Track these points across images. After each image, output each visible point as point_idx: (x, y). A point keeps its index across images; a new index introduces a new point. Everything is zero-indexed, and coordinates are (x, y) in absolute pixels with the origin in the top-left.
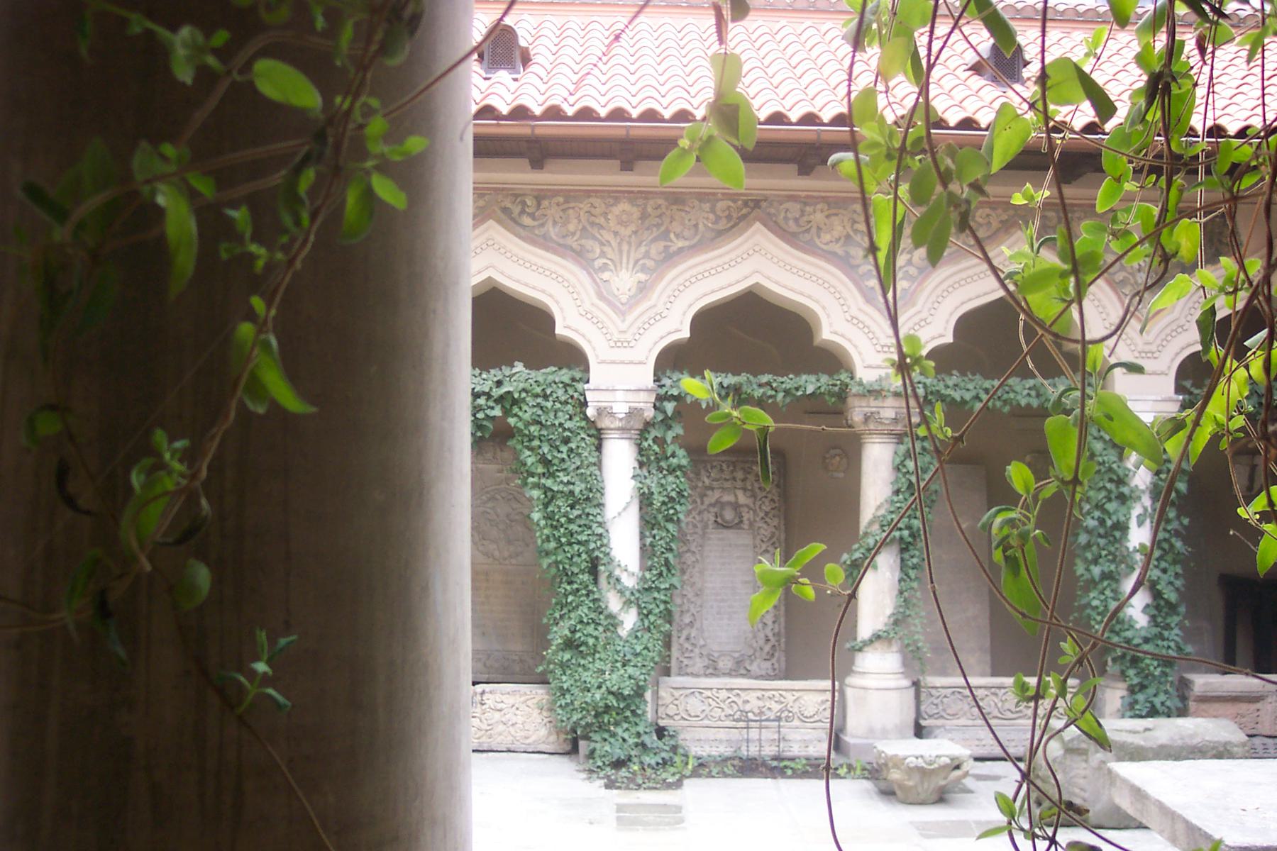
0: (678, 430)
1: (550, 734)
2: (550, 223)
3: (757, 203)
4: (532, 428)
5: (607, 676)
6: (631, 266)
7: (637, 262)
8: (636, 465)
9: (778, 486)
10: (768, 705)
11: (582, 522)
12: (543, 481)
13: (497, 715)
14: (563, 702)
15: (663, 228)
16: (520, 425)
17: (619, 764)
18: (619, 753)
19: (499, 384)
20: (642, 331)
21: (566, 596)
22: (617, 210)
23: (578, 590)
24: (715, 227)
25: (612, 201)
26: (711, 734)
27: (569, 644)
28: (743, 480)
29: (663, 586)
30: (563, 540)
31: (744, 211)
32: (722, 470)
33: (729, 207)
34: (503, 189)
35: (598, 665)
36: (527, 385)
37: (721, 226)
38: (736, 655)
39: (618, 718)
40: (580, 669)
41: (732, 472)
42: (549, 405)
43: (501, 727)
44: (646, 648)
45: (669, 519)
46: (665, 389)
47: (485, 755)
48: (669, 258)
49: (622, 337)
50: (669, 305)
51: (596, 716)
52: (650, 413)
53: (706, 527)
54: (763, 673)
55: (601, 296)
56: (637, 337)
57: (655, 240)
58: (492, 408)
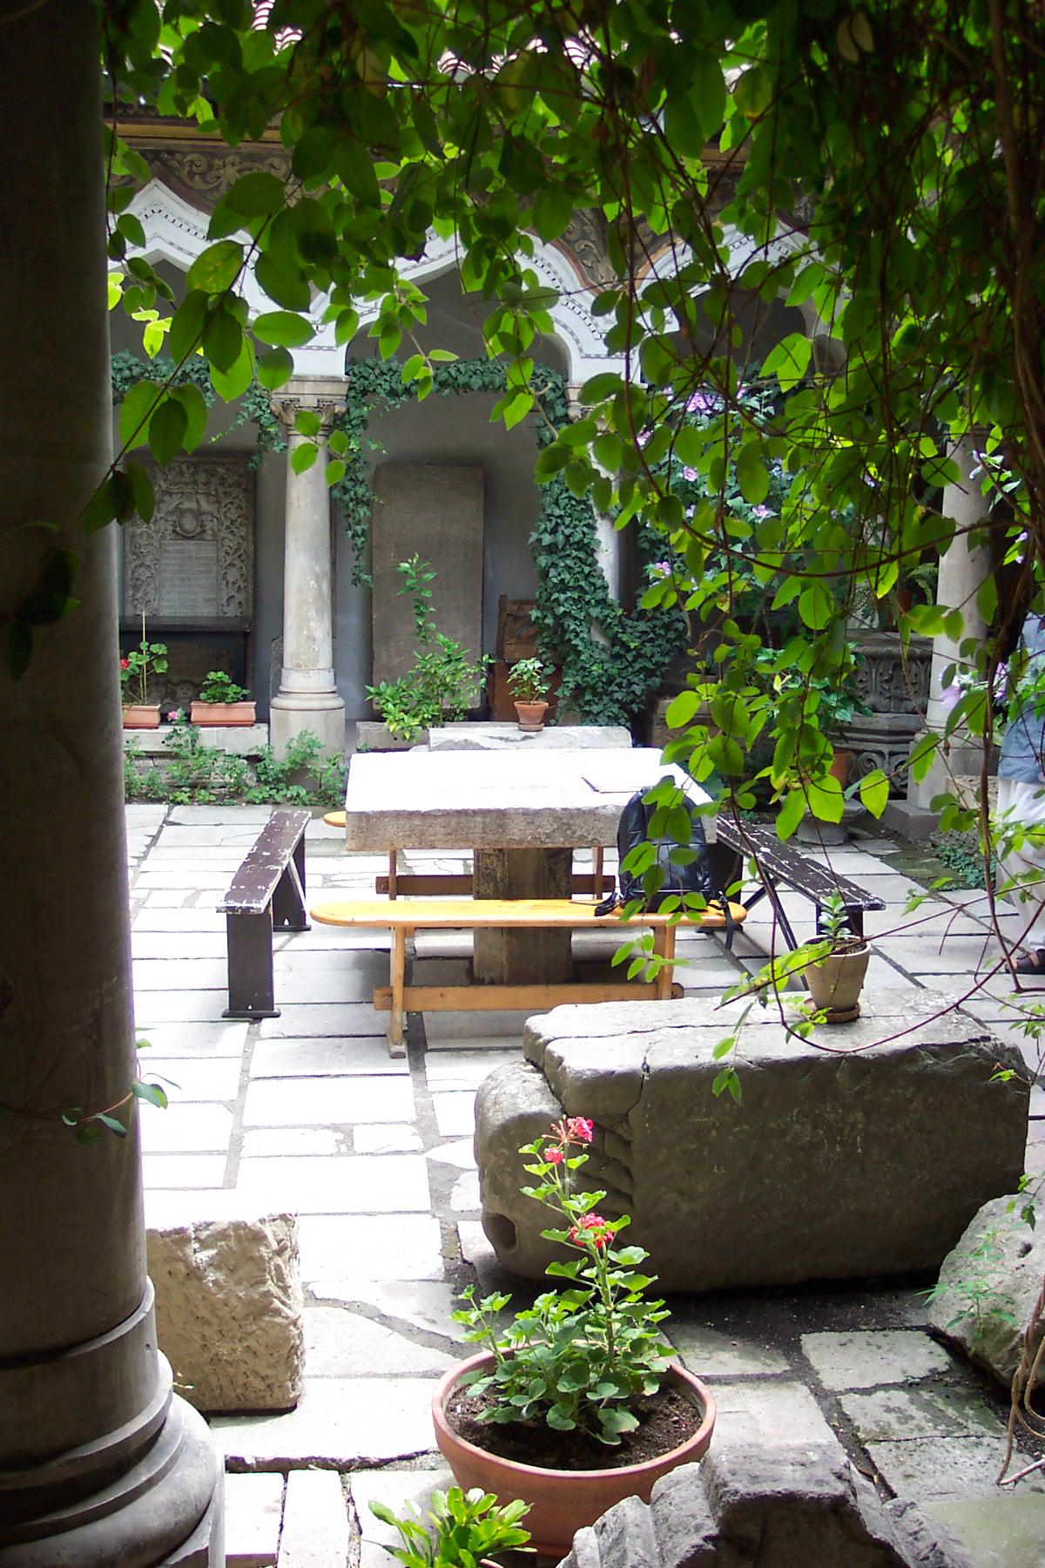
32: (181, 473)
53: (163, 537)
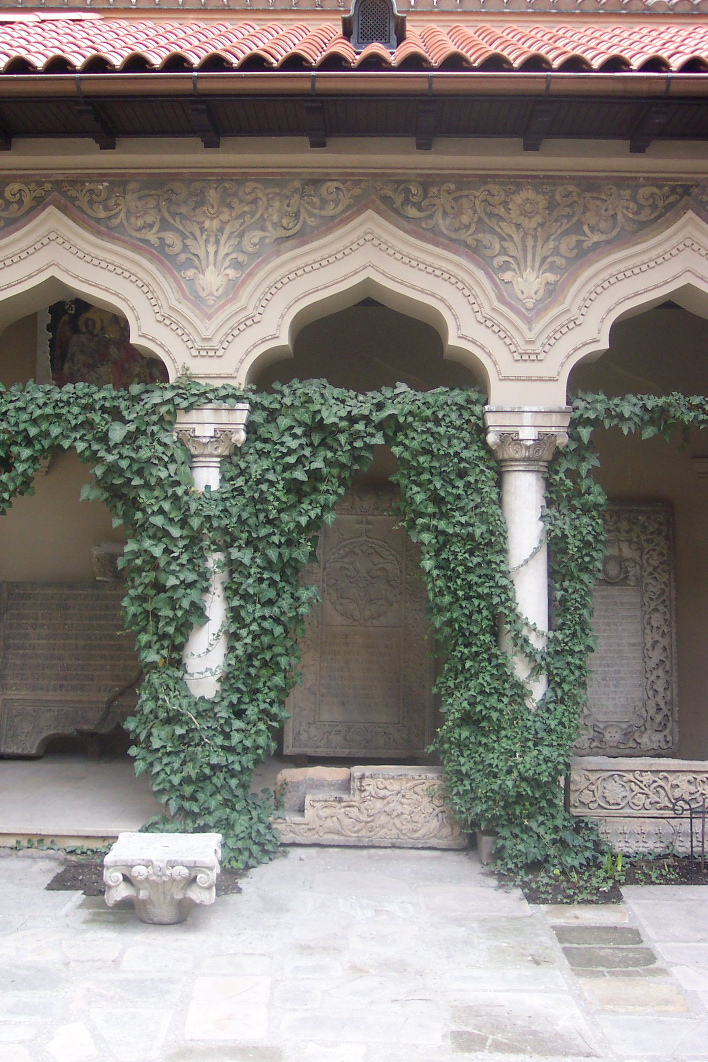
0: (594, 461)
1: (442, 826)
2: (439, 215)
3: (686, 190)
4: (421, 459)
5: (518, 759)
6: (537, 265)
7: (544, 259)
8: (544, 504)
9: (667, 538)
10: (701, 790)
11: (484, 572)
12: (435, 522)
13: (379, 804)
14: (461, 789)
15: (574, 220)
16: (407, 455)
17: (534, 866)
18: (536, 853)
19: (380, 406)
20: (552, 341)
21: (462, 661)
22: (519, 199)
23: (477, 654)
24: (636, 218)
25: (513, 188)
26: (635, 825)
27: (467, 719)
28: (628, 532)
29: (577, 649)
30: (461, 593)
31: (672, 199)
33: (652, 195)
34: (383, 175)
35: (505, 743)
36: (413, 408)
37: (643, 217)
38: (624, 726)
39: (532, 809)
40: (481, 749)
41: (616, 522)
42: (442, 430)
43: (384, 819)
44: (561, 723)
45: (584, 568)
46: (579, 413)
47: (364, 852)
48: (583, 255)
49: (530, 348)
50: (584, 310)
51: (504, 808)
52: (563, 440)
54: (655, 746)
55: (502, 299)
56: (547, 348)
57: (566, 233)
58: (372, 435)
